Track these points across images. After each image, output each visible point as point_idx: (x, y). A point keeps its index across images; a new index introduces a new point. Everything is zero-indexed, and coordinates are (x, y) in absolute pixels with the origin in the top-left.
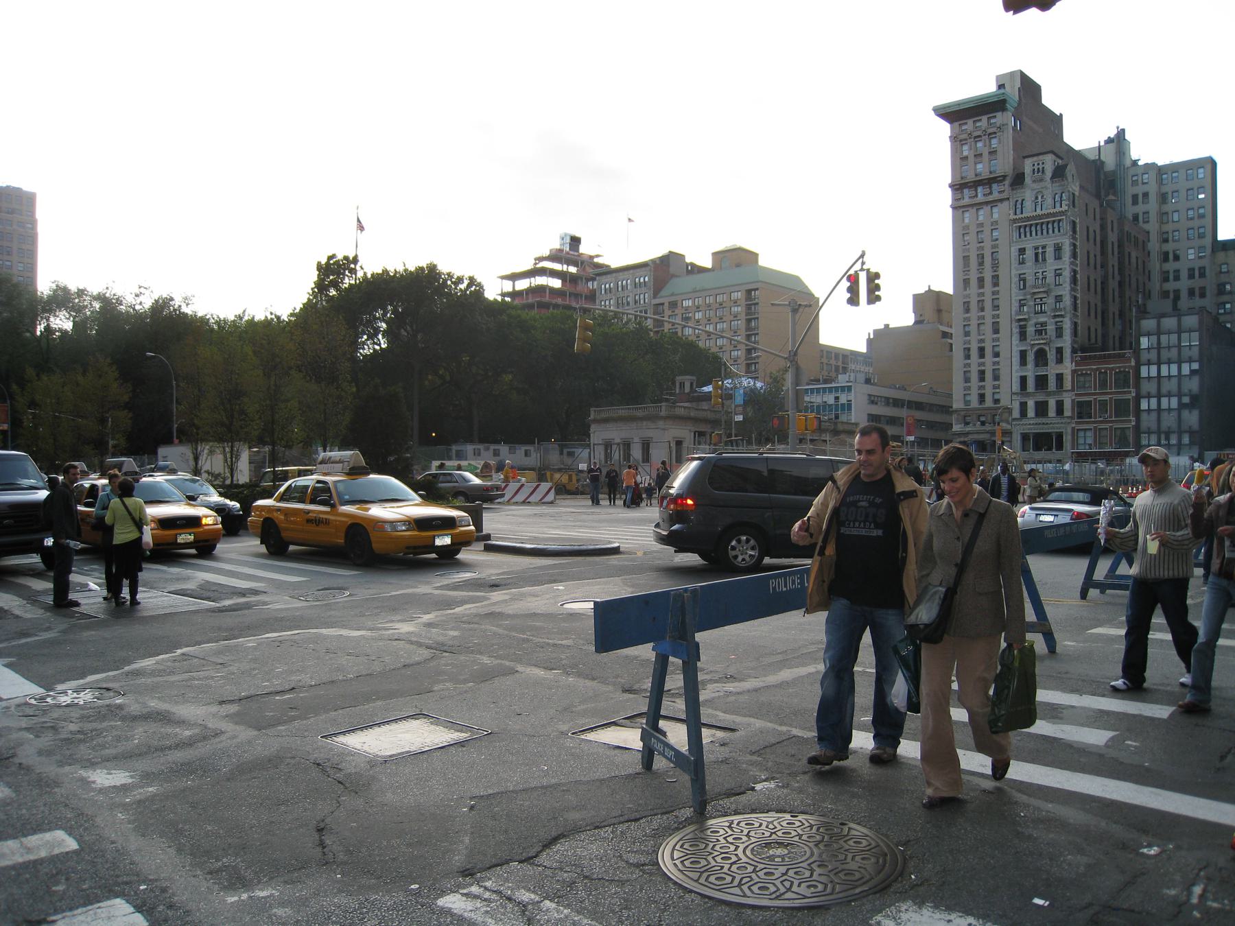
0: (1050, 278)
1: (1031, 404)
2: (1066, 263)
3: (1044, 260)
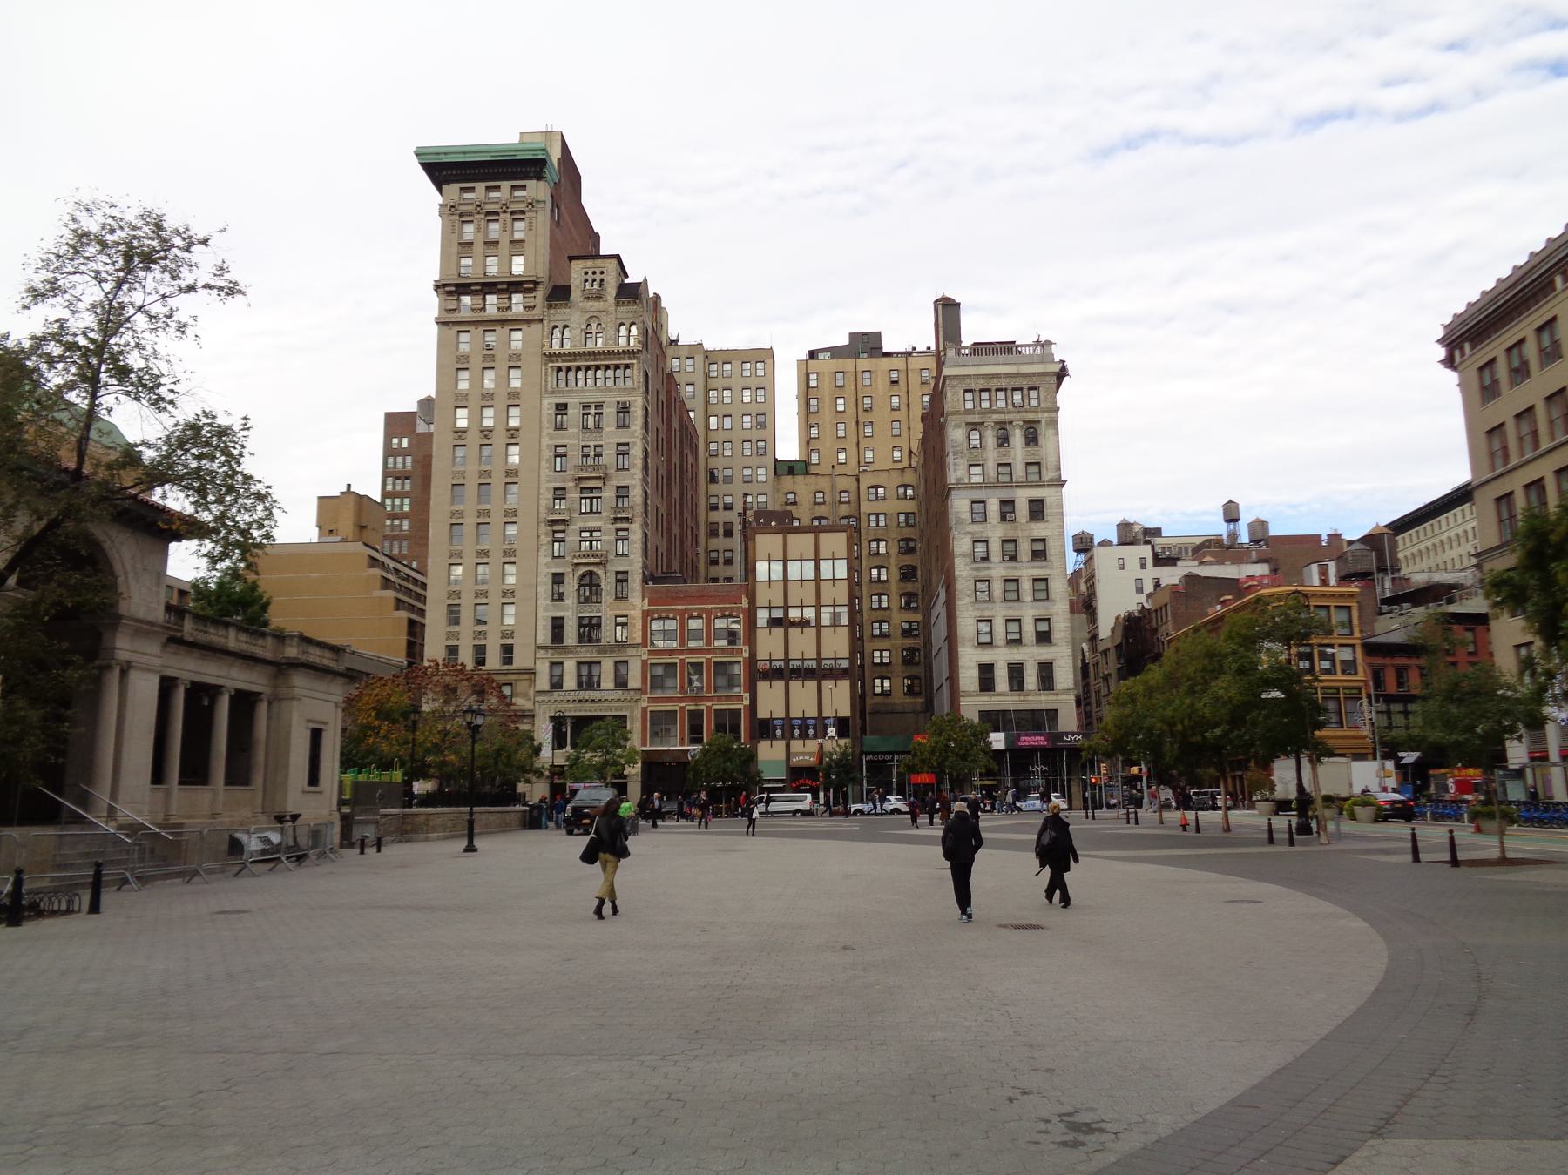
0: (609, 456)
1: (570, 666)
2: (635, 435)
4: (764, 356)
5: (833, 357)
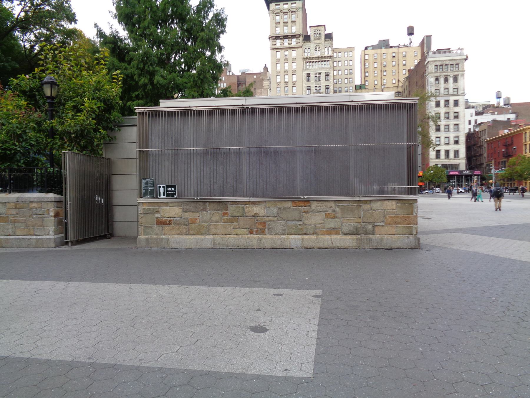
4: (351, 50)
5: (372, 49)
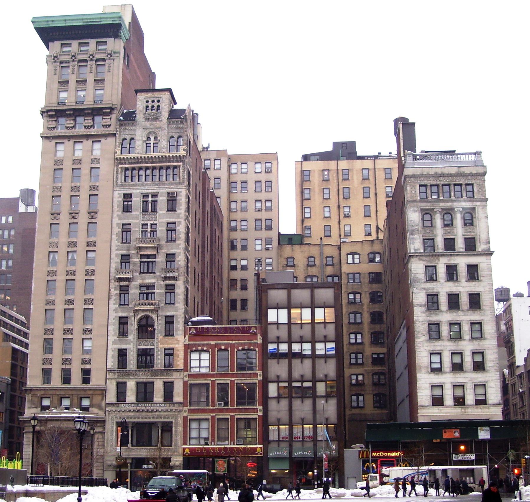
1: (131, 385)
2: (180, 216)
3: (154, 210)
